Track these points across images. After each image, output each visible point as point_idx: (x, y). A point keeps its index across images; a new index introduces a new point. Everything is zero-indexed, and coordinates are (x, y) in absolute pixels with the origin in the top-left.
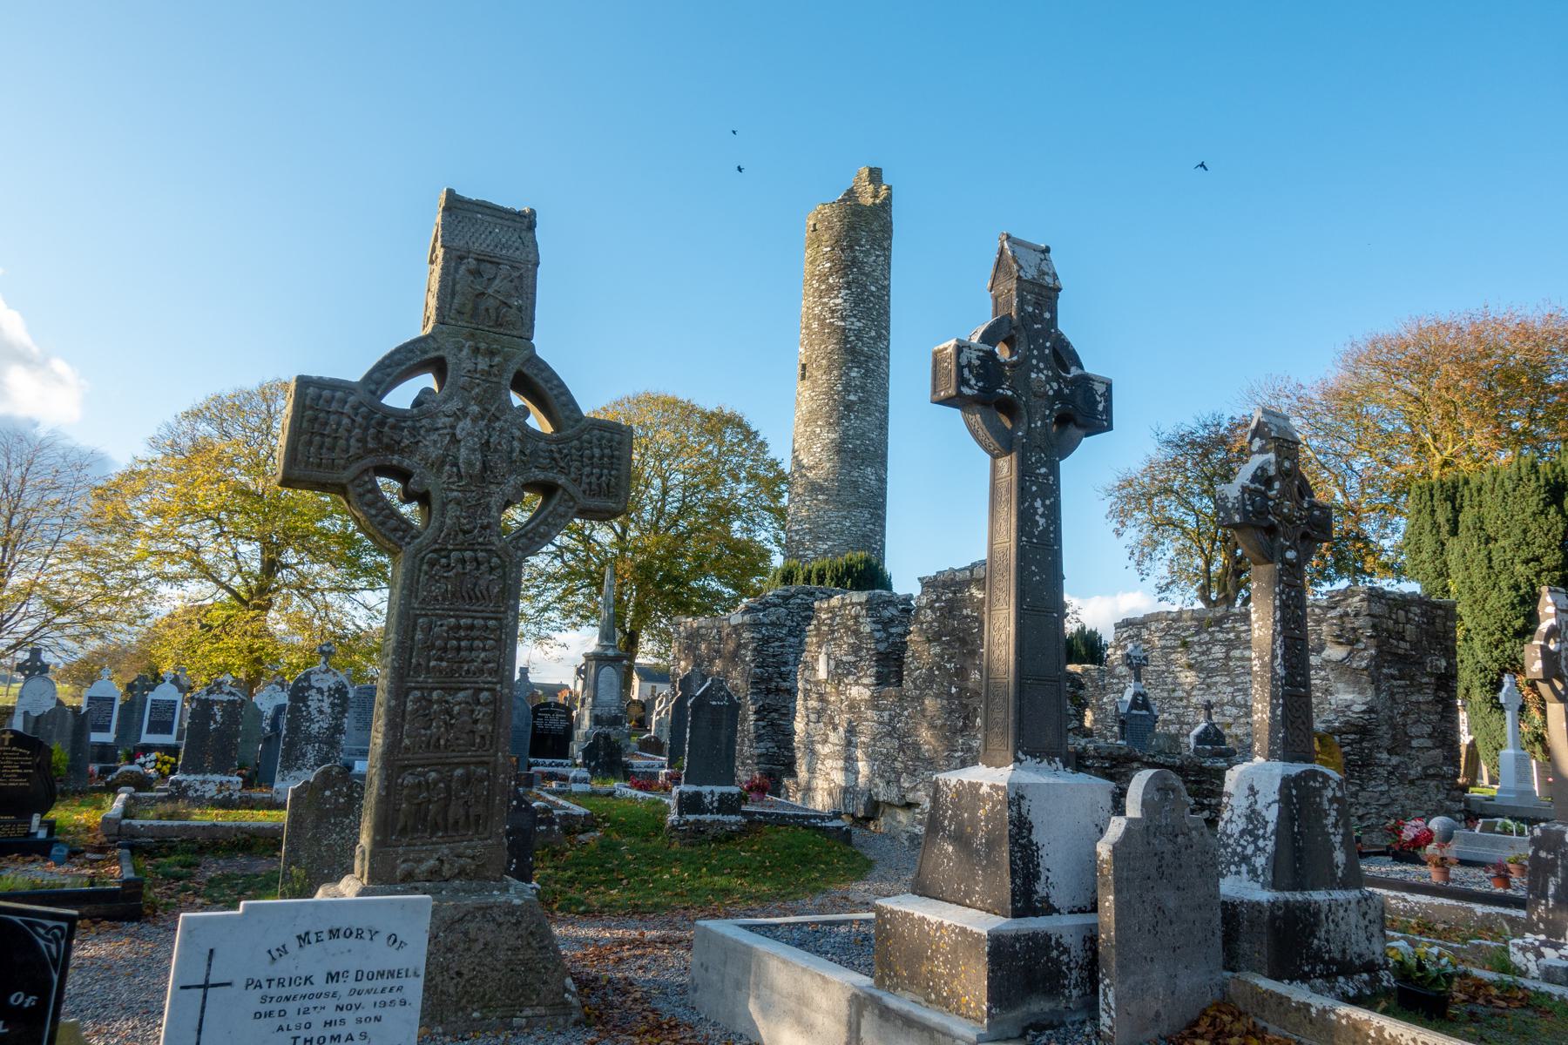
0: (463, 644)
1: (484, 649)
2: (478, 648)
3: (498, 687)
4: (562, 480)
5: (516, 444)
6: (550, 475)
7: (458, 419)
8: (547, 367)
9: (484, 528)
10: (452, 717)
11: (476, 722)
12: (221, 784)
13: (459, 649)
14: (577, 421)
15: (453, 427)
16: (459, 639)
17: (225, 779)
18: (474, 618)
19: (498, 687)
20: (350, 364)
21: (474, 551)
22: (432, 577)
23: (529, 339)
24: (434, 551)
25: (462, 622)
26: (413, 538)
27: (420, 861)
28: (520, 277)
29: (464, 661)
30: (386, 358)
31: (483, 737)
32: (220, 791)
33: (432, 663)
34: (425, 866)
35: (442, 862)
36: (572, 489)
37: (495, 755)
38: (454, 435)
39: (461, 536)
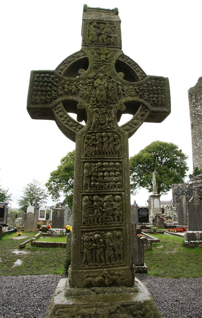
0: (105, 174)
1: (116, 176)
2: (112, 176)
3: (123, 193)
4: (142, 100)
5: (120, 86)
6: (136, 99)
7: (95, 80)
8: (129, 58)
9: (109, 122)
10: (103, 208)
11: (114, 210)
12: (61, 231)
13: (103, 176)
14: (144, 77)
15: (93, 83)
16: (103, 172)
17: (62, 229)
18: (109, 162)
19: (123, 193)
20: (51, 64)
21: (107, 132)
22: (89, 145)
23: (121, 48)
24: (89, 134)
25: (104, 164)
26: (80, 129)
27: (95, 277)
28: (114, 27)
29: (107, 182)
30: (65, 60)
31: (118, 217)
32: (61, 233)
33: (92, 183)
34: (97, 279)
35: (104, 277)
36: (146, 103)
37: (125, 226)
38: (93, 86)
39: (100, 126)
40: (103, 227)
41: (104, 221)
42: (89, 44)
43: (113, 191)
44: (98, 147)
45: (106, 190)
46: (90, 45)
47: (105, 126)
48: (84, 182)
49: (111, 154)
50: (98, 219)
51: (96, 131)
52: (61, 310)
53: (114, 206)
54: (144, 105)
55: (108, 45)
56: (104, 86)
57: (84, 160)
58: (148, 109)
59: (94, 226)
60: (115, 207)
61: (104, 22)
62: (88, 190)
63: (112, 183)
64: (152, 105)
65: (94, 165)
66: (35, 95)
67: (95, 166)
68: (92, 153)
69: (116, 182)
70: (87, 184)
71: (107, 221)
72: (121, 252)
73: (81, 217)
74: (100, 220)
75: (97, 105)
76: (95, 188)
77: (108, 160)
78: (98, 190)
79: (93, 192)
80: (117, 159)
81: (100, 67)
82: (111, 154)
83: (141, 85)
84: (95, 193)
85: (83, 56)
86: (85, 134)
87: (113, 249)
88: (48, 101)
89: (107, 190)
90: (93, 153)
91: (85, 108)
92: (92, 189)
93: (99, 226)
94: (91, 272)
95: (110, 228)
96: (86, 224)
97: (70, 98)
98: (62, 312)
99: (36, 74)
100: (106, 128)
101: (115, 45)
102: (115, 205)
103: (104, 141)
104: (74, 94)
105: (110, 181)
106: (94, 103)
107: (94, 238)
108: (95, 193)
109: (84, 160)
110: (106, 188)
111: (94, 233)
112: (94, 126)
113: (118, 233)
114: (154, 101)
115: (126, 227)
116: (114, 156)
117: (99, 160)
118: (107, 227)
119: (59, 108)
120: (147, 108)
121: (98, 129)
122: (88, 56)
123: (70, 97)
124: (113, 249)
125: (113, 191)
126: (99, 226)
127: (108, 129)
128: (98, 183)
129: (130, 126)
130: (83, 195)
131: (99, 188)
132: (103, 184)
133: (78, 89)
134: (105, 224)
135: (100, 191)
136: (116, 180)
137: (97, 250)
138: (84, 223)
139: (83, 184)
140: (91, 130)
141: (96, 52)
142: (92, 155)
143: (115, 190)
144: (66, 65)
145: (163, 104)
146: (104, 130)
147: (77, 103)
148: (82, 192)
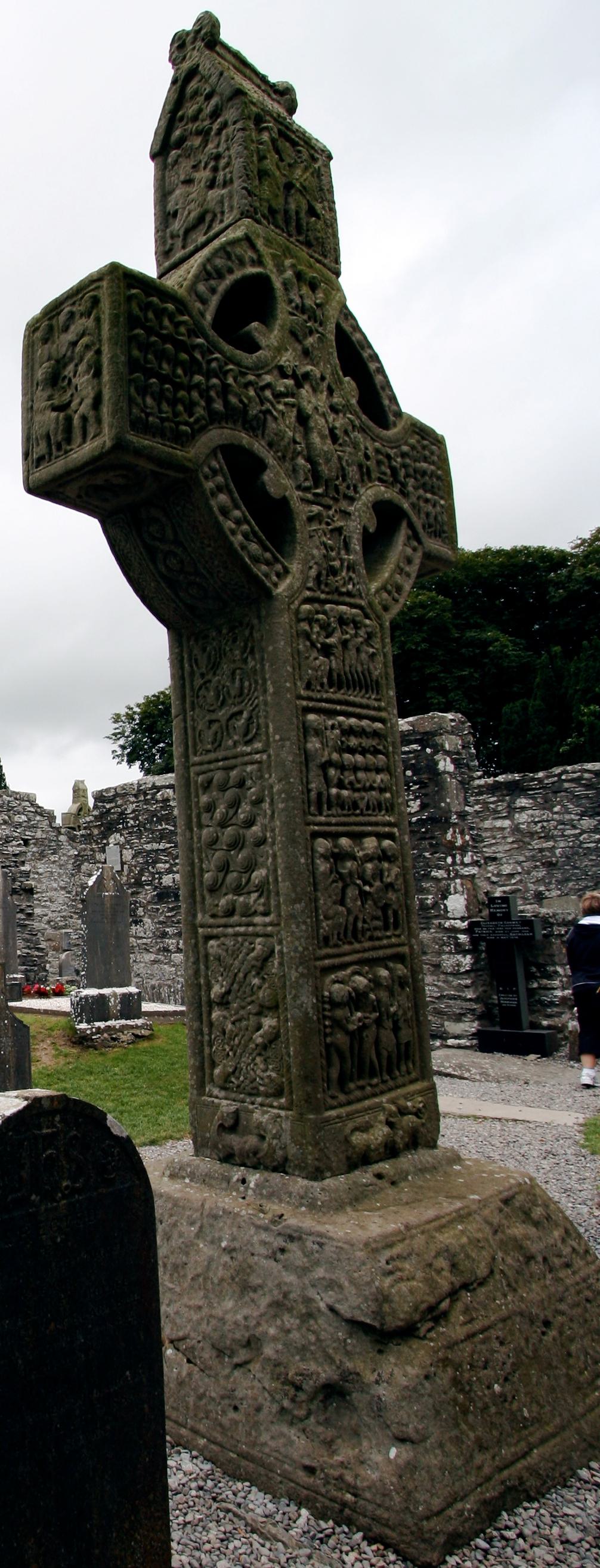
11: (390, 886)
40: (365, 951)
41: (369, 930)
42: (264, 216)
43: (376, 824)
44: (336, 658)
45: (361, 819)
46: (265, 222)
47: (341, 582)
48: (313, 786)
49: (363, 691)
50: (356, 919)
51: (323, 596)
52: (388, 1253)
53: (386, 874)
54: (411, 526)
55: (308, 244)
56: (327, 421)
57: (305, 703)
58: (420, 542)
59: (346, 948)
60: (389, 880)
61: (293, 137)
62: (321, 814)
63: (374, 793)
64: (424, 527)
65: (330, 723)
66: (143, 391)
67: (333, 727)
68: (322, 677)
69: (382, 790)
70: (319, 795)
71: (376, 929)
72: (405, 1034)
73: (317, 916)
74: (360, 925)
75: (315, 494)
76: (340, 811)
77: (358, 710)
78: (344, 815)
79: (337, 824)
80: (374, 709)
81: (305, 337)
82: (363, 691)
83: (395, 443)
84: (341, 829)
85: (253, 263)
86: (296, 602)
87: (395, 1023)
88: (185, 433)
89: (366, 819)
90: (325, 680)
91: (287, 494)
92: (334, 811)
93: (357, 946)
94: (358, 1112)
95: (381, 953)
96: (331, 943)
97: (244, 442)
98: (392, 1259)
99: (130, 286)
100: (344, 590)
101: (325, 257)
102: (389, 870)
103: (348, 636)
104: (256, 426)
105: (372, 788)
106: (307, 484)
107: (354, 989)
108: (341, 829)
109: (305, 703)
110: (362, 810)
111: (349, 971)
112: (319, 575)
113: (401, 969)
114: (428, 515)
115: (411, 947)
116: (369, 698)
117: (338, 708)
118: (374, 949)
119: (215, 472)
120: (416, 536)
121: (327, 590)
122: (269, 273)
123: (244, 439)
124: (395, 1023)
125: (376, 824)
126: (357, 946)
127: (349, 594)
128: (345, 793)
129: (389, 593)
130: (315, 835)
131: (349, 810)
132: (356, 795)
133: (263, 408)
134: (371, 939)
135: (353, 819)
136: (382, 786)
137: (364, 1034)
138: (326, 940)
139: (309, 791)
140: (309, 589)
141: (293, 266)
142: (322, 685)
143: (380, 818)
144: (213, 282)
145: (444, 532)
146: (341, 594)
147: (262, 466)
148: (308, 824)
